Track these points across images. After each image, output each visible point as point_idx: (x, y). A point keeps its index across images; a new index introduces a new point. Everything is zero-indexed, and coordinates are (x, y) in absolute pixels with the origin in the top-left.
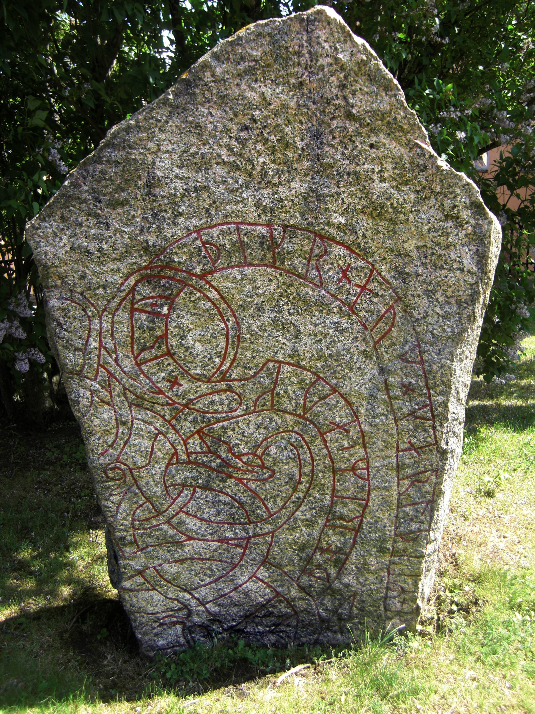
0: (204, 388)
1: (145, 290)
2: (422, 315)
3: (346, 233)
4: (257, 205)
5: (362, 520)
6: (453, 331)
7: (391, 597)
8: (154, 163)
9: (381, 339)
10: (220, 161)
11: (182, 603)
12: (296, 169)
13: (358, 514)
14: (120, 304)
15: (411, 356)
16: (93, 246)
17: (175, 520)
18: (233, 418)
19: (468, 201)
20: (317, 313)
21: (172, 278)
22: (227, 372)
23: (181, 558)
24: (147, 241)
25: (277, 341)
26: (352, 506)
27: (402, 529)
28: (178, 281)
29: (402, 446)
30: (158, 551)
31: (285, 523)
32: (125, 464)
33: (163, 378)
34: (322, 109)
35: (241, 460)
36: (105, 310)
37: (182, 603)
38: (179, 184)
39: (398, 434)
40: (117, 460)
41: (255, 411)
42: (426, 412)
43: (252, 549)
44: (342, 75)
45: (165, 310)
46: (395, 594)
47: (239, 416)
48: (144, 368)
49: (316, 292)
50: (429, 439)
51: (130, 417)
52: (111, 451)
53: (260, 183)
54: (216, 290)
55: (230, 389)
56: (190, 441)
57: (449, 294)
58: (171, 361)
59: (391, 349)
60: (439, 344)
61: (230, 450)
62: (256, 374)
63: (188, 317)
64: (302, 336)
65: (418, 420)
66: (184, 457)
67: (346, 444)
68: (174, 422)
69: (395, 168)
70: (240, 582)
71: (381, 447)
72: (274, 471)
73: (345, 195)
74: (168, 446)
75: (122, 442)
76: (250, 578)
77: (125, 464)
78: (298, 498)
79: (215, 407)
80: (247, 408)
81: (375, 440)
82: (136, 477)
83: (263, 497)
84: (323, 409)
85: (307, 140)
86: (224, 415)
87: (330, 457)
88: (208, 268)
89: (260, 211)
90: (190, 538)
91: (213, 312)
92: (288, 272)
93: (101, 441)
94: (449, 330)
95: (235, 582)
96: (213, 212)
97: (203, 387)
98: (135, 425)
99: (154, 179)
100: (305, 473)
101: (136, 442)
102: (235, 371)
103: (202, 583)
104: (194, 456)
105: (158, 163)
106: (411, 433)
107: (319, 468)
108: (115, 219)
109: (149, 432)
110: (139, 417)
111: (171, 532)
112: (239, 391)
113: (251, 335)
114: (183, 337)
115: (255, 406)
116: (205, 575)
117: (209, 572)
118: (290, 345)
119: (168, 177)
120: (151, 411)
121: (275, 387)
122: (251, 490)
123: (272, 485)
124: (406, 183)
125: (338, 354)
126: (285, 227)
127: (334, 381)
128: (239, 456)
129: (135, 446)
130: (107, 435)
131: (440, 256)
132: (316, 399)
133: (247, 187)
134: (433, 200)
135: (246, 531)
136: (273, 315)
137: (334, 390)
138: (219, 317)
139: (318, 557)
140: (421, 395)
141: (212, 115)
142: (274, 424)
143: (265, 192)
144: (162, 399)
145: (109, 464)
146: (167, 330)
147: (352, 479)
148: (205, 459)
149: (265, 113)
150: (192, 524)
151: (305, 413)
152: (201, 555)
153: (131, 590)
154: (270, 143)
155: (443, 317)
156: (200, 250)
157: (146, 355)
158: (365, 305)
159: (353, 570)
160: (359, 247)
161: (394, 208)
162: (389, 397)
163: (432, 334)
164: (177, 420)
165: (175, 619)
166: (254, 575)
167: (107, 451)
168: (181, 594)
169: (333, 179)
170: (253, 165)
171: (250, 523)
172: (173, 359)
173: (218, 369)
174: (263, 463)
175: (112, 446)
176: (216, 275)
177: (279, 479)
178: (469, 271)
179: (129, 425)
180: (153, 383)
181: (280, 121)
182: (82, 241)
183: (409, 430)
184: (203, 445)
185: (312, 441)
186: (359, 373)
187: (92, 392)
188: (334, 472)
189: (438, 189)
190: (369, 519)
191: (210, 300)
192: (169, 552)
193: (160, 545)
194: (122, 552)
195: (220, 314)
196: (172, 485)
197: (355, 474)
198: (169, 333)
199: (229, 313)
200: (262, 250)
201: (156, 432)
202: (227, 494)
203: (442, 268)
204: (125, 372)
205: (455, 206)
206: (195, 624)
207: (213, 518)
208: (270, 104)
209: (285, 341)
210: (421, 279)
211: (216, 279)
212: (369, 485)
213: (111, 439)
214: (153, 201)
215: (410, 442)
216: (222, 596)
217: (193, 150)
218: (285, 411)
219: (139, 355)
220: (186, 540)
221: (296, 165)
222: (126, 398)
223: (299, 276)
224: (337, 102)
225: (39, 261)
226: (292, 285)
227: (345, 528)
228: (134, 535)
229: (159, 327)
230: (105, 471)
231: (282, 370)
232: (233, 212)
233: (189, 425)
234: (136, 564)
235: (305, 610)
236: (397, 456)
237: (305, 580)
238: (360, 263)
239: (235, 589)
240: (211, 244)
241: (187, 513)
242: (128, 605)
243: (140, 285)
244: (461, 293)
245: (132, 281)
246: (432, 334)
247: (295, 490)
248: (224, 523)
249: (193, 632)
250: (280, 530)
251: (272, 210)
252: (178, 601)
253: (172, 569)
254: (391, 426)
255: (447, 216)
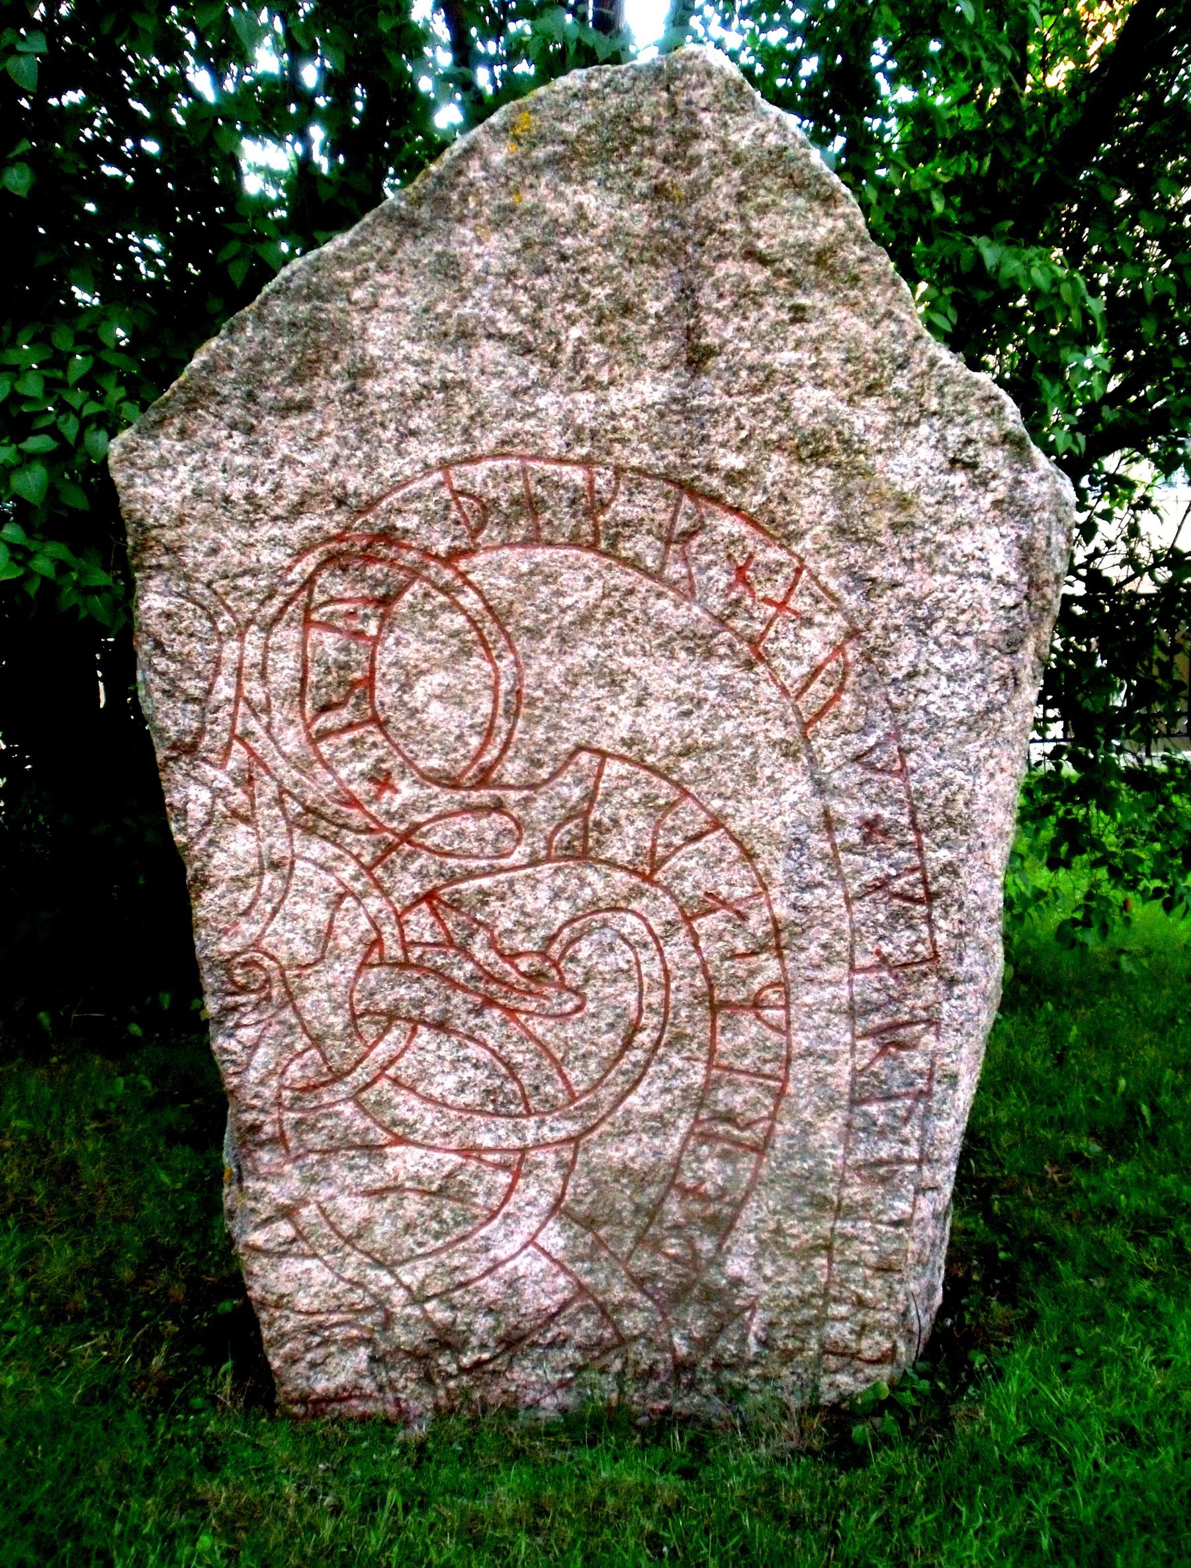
0: (445, 799)
1: (334, 584)
2: (904, 671)
3: (744, 490)
4: (567, 422)
5: (772, 1128)
6: (969, 709)
7: (835, 1319)
8: (364, 330)
9: (819, 715)
10: (492, 330)
11: (373, 1296)
12: (644, 356)
13: (765, 1113)
14: (282, 611)
15: (881, 758)
16: (237, 489)
17: (370, 1096)
18: (502, 870)
19: (996, 433)
20: (683, 655)
21: (392, 562)
22: (492, 767)
23: (378, 1185)
24: (342, 484)
25: (599, 709)
26: (752, 1092)
27: (860, 1156)
28: (402, 568)
29: (863, 961)
30: (328, 1167)
31: (603, 1119)
32: (272, 958)
33: (362, 774)
34: (697, 238)
35: (516, 967)
36: (250, 622)
37: (373, 1296)
38: (411, 373)
39: (854, 931)
40: (255, 945)
41: (548, 859)
42: (913, 885)
43: (531, 1179)
44: (736, 174)
45: (372, 628)
46: (843, 1310)
47: (514, 868)
48: (324, 748)
49: (682, 610)
50: (919, 948)
51: (288, 854)
52: (244, 926)
53: (571, 379)
54: (479, 592)
55: (499, 807)
56: (411, 917)
57: (960, 627)
58: (379, 738)
59: (839, 741)
60: (941, 735)
61: (492, 944)
62: (554, 775)
63: (415, 645)
64: (649, 702)
65: (896, 901)
66: (396, 952)
67: (740, 946)
68: (379, 872)
69: (847, 361)
70: (502, 1255)
71: (816, 961)
72: (583, 997)
73: (744, 410)
74: (364, 924)
75: (268, 908)
76: (525, 1247)
77: (272, 958)
78: (635, 1064)
79: (465, 845)
80: (534, 853)
81: (802, 942)
82: (293, 988)
83: (559, 1056)
84: (691, 864)
85: (666, 301)
86: (483, 863)
87: (705, 972)
88: (461, 544)
89: (570, 435)
90: (400, 1140)
91: (469, 637)
92: (625, 562)
93: (224, 902)
94: (961, 705)
95: (491, 1254)
96: (477, 433)
97: (444, 797)
98: (297, 872)
99: (362, 360)
100: (649, 1006)
101: (298, 910)
102: (509, 766)
103: (420, 1251)
104: (418, 951)
105: (371, 330)
106: (881, 931)
107: (681, 996)
108: (282, 436)
109: (326, 890)
110: (307, 854)
111: (360, 1123)
112: (516, 812)
113: (546, 692)
114: (406, 687)
115: (548, 847)
116: (426, 1231)
117: (435, 1226)
118: (626, 719)
119: (391, 359)
120: (334, 843)
121: (591, 806)
122: (532, 1037)
123: (580, 1029)
124: (870, 390)
125: (725, 743)
126: (619, 471)
127: (717, 804)
128: (512, 957)
129: (295, 918)
130: (239, 890)
131: (940, 546)
132: (677, 840)
133: (547, 386)
134: (924, 429)
135: (517, 1129)
136: (592, 652)
137: (717, 822)
138: (481, 650)
139: (674, 1207)
140: (902, 845)
141: (480, 243)
142: (588, 891)
143: (581, 397)
144: (357, 818)
145: (237, 954)
146: (372, 670)
147: (754, 1029)
148: (440, 961)
149: (586, 242)
150: (406, 1107)
151: (653, 871)
152: (420, 1182)
153: (267, 1253)
154: (592, 302)
155: (950, 678)
156: (447, 508)
157: (329, 721)
158: (784, 644)
159: (749, 1246)
160: (772, 521)
161: (847, 442)
162: (834, 845)
163: (927, 712)
164: (385, 867)
165: (355, 1332)
166: (532, 1241)
167: (236, 924)
168: (371, 1273)
169: (718, 378)
170: (559, 344)
171: (529, 1113)
172: (384, 733)
173: (474, 760)
174: (562, 978)
175: (245, 913)
176: (480, 559)
177: (593, 1015)
178: (1001, 580)
179: (286, 871)
180: (340, 782)
181: (612, 260)
182: (216, 478)
183: (876, 923)
184: (439, 930)
185: (668, 935)
186: (768, 790)
187: (217, 793)
188: (715, 1008)
189: (934, 405)
190: (788, 1126)
191: (464, 612)
192: (351, 1168)
193: (335, 1150)
194: (254, 1161)
195: (484, 643)
196: (367, 1012)
197: (758, 1017)
198: (378, 676)
199: (502, 643)
200: (574, 516)
201: (340, 890)
202: (484, 1044)
203: (945, 571)
204: (284, 755)
205: (969, 442)
206: (398, 1349)
207: (450, 1099)
208: (593, 226)
209: (615, 709)
210: (901, 592)
211: (478, 567)
212: (789, 1046)
213: (245, 899)
214: (360, 404)
215: (878, 953)
216: (461, 1285)
217: (442, 307)
218: (612, 863)
219: (315, 719)
220: (390, 1144)
221: (643, 349)
222: (284, 810)
223: (646, 572)
224: (728, 227)
225: (130, 513)
226: (631, 592)
227: (738, 1143)
228: (280, 1121)
229: (359, 663)
230: (229, 971)
231: (607, 771)
232: (516, 434)
233: (410, 880)
234: (277, 1192)
235: (643, 1334)
236: (850, 983)
237: (643, 1261)
238: (774, 554)
239: (489, 1272)
240: (471, 496)
241: (396, 1081)
242: (257, 1287)
243: (325, 574)
244: (986, 626)
245: (309, 563)
246: (927, 712)
247: (628, 1044)
248: (474, 1111)
249: (393, 1368)
250: (594, 1136)
251: (594, 434)
252: (365, 1289)
253: (355, 1210)
254: (837, 911)
255: (953, 461)
